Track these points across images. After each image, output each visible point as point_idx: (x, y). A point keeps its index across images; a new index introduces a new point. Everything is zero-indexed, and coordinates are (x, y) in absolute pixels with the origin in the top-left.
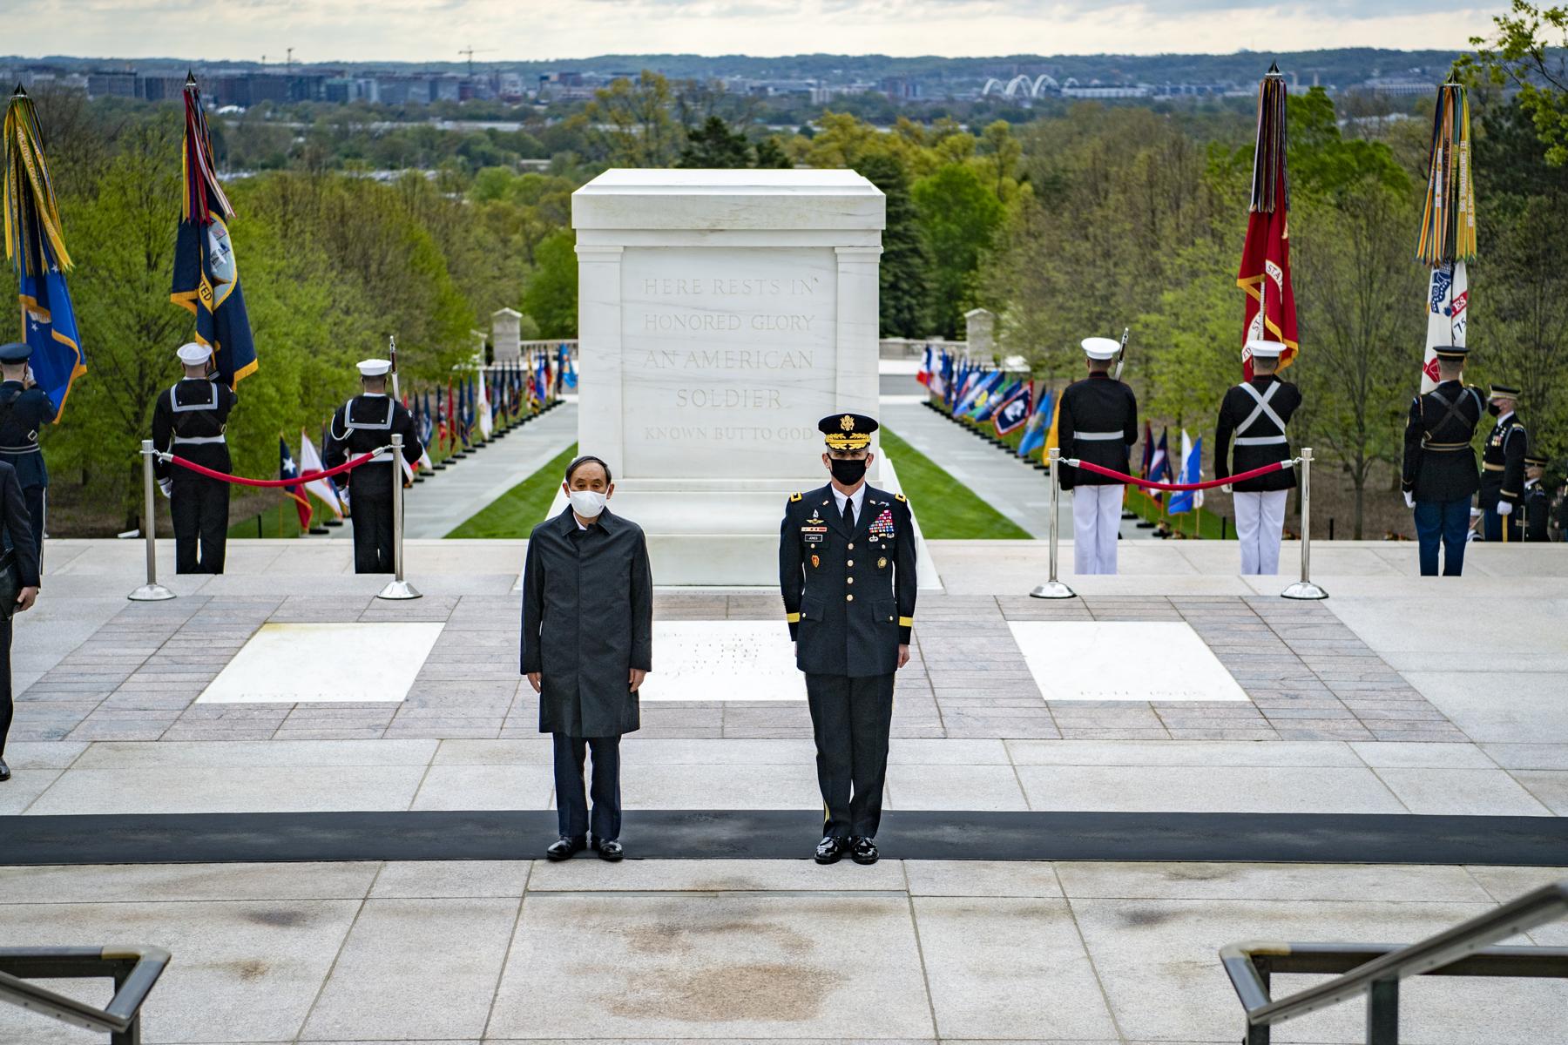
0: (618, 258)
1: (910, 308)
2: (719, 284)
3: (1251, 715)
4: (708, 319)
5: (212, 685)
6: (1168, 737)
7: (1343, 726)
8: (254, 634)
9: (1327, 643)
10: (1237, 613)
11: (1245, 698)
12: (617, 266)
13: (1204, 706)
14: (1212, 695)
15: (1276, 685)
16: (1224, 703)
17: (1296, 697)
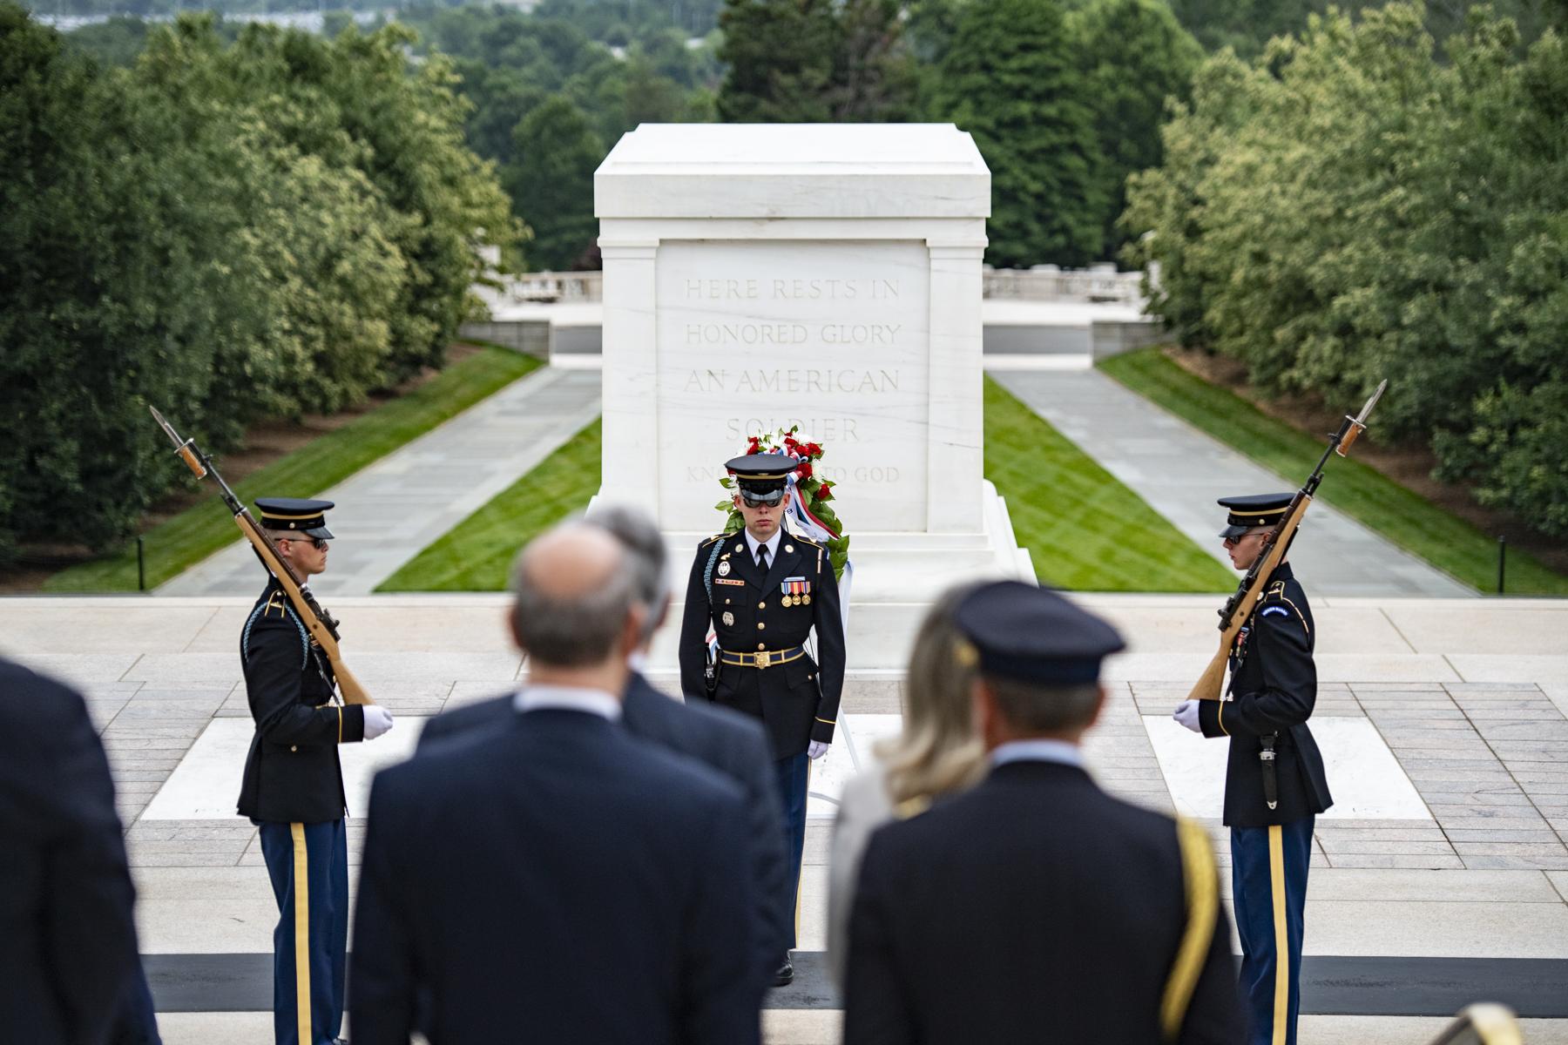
0: (653, 254)
1: (1065, 230)
2: (779, 286)
3: (1432, 838)
4: (767, 330)
5: (157, 798)
6: (1326, 864)
7: (1543, 852)
8: (202, 731)
9: (1541, 745)
10: (1434, 705)
11: (1428, 816)
12: (652, 263)
13: (1376, 825)
14: (1390, 812)
15: (1469, 800)
16: (1401, 822)
17: (1491, 815)
